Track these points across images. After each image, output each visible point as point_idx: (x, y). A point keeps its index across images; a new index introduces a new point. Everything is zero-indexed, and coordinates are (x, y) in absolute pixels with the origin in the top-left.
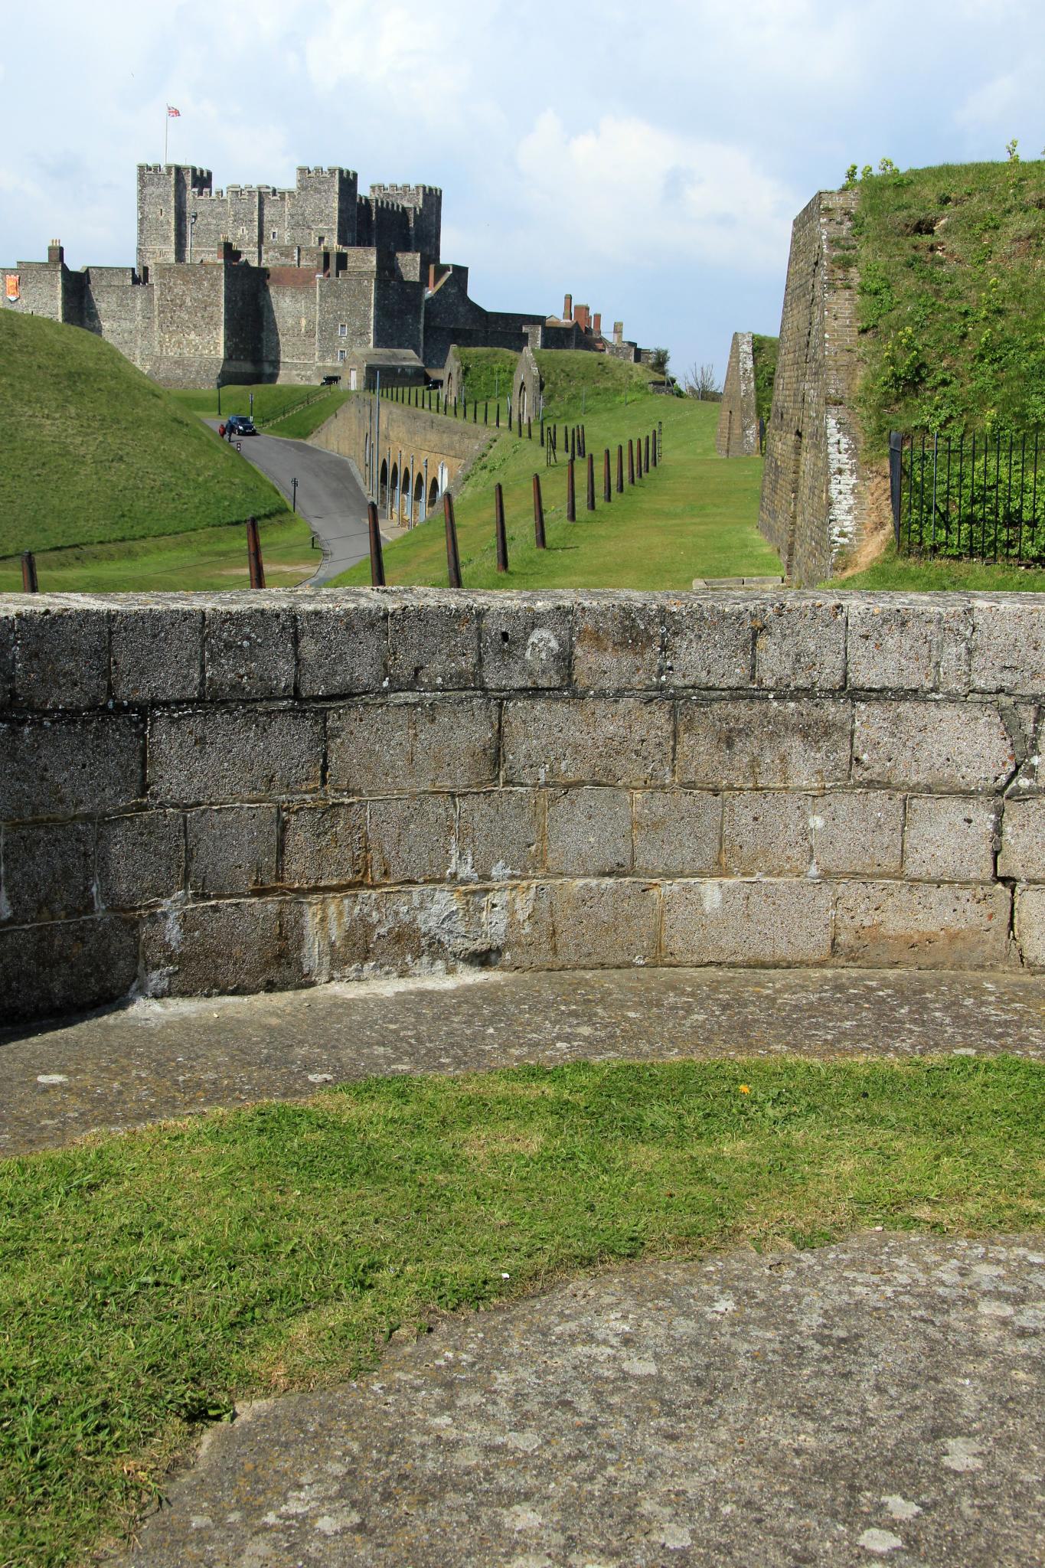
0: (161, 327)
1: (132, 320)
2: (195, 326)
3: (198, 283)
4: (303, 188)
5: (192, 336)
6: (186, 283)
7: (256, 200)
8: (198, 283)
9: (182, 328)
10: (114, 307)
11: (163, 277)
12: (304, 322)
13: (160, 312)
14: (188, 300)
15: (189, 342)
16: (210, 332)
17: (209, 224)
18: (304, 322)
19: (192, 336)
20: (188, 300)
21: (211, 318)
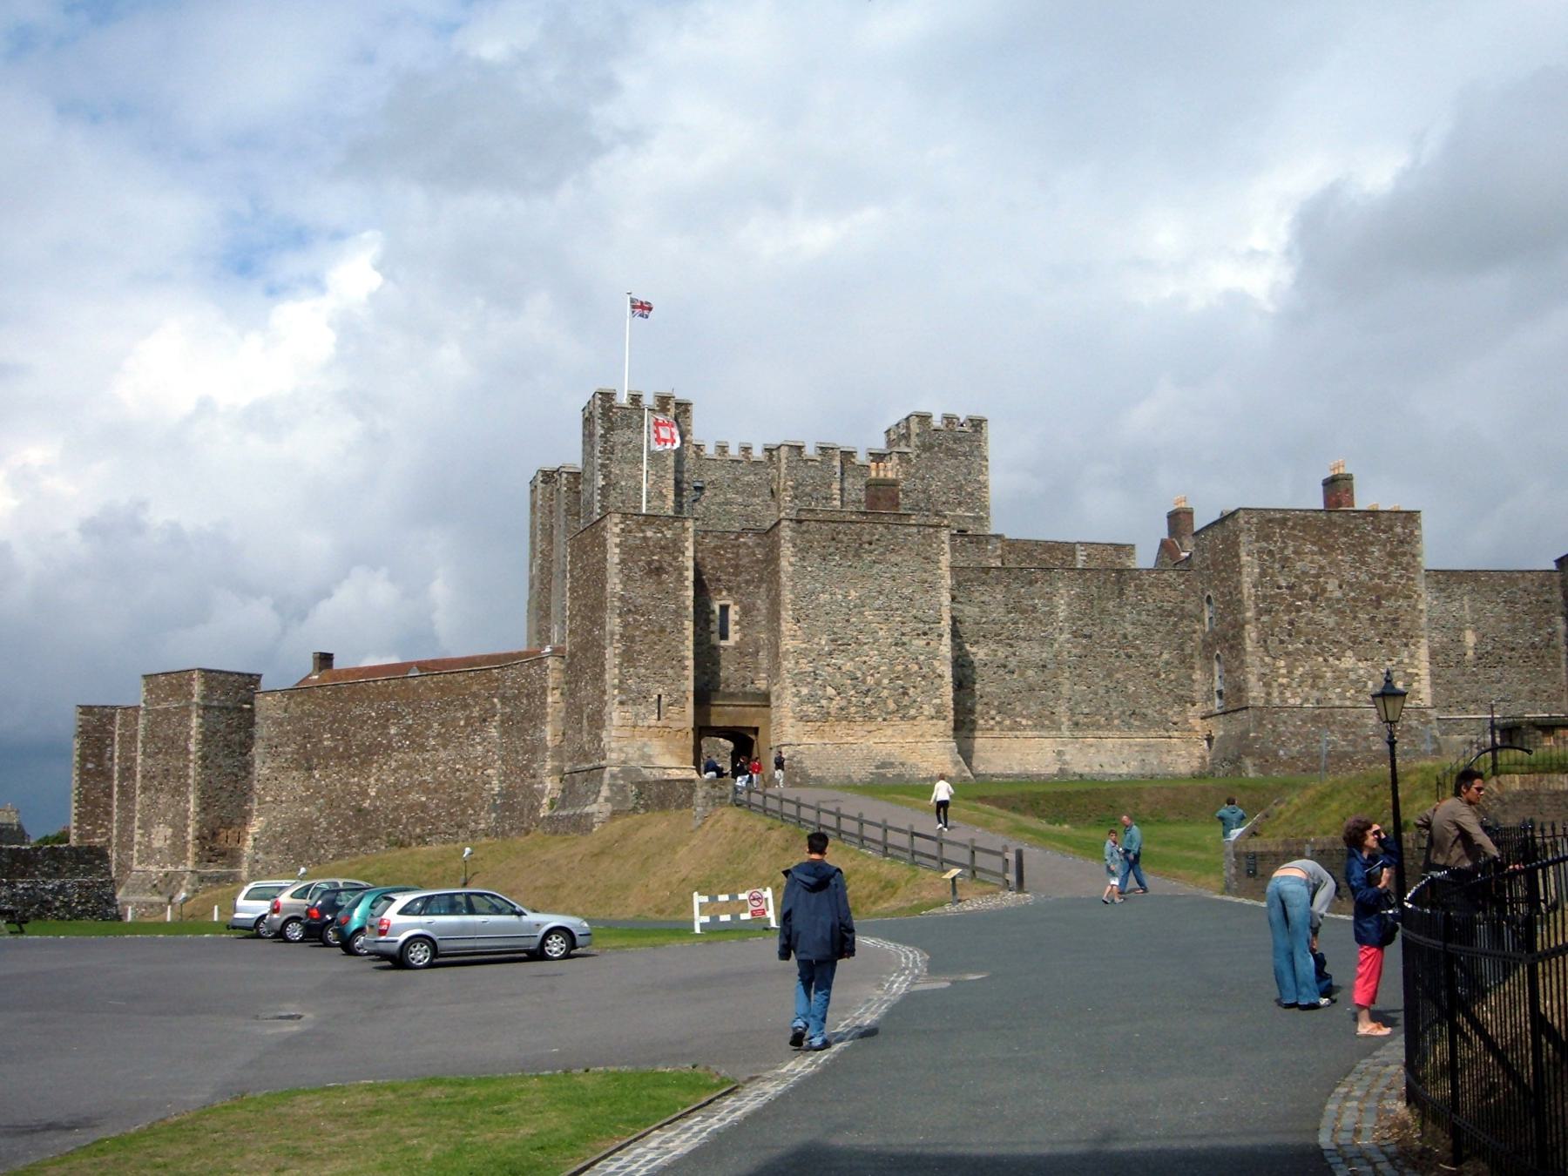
0: (1263, 642)
1: (1046, 641)
2: (1355, 641)
3: (1360, 551)
4: (926, 447)
5: (1348, 661)
6: (1327, 549)
7: (837, 463)
8: (1360, 551)
9: (1322, 643)
10: (998, 613)
11: (1267, 538)
12: (1470, 638)
13: (1260, 612)
14: (1332, 585)
15: (1340, 676)
16: (1393, 651)
17: (728, 502)
18: (1470, 638)
19: (1348, 661)
20: (1332, 585)
21: (1395, 622)
